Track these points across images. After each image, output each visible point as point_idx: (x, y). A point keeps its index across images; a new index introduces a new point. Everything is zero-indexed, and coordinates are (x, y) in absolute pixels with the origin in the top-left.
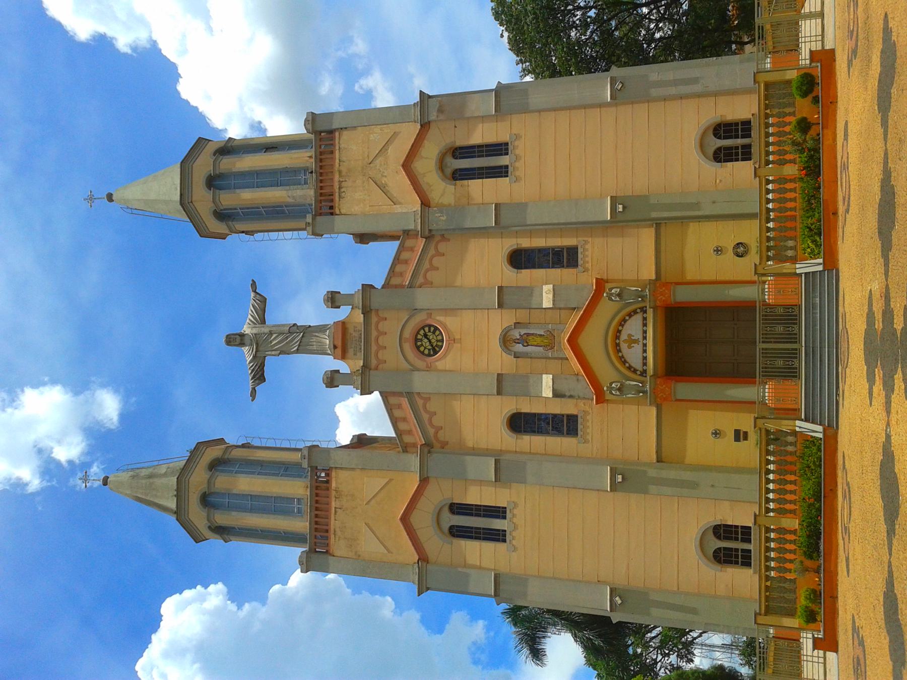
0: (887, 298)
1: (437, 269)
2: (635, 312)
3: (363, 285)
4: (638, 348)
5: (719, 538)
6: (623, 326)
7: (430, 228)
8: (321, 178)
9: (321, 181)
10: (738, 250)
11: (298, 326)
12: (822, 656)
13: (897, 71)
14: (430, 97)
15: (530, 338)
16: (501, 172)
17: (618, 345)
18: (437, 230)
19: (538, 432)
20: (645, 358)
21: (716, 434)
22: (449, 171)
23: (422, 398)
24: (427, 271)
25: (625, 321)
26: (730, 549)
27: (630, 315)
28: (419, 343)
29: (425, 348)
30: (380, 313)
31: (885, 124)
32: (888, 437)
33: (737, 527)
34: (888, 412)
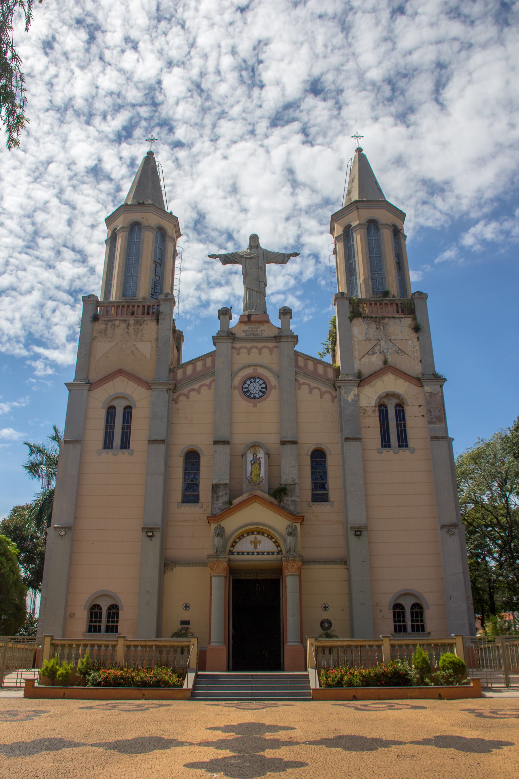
0: (290, 743)
1: (310, 393)
2: (278, 546)
3: (297, 336)
4: (250, 548)
5: (109, 609)
6: (268, 537)
7: (342, 387)
8: (378, 304)
9: (376, 304)
10: (326, 623)
11: (265, 288)
12: (22, 686)
13: (469, 753)
14: (441, 386)
15: (258, 466)
16: (386, 443)
17: (253, 533)
18: (340, 393)
19: (185, 473)
20: (243, 554)
21: (186, 607)
22: (386, 401)
23: (211, 383)
24: (309, 385)
25: (271, 538)
26: (101, 617)
27: (275, 542)
28: (252, 380)
29: (249, 385)
30: (275, 350)
31: (426, 742)
32: (182, 744)
33: (117, 622)
34: (200, 744)
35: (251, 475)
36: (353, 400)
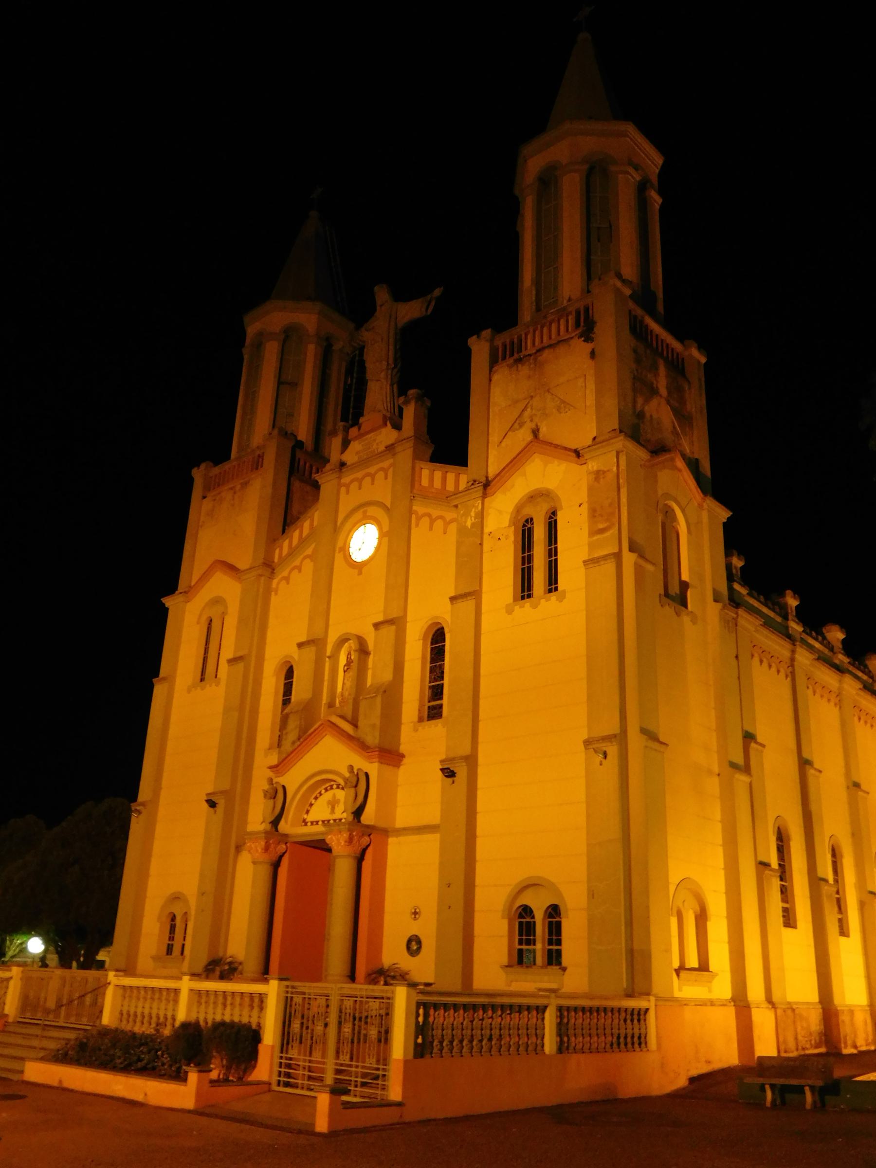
7: (459, 506)
35: (343, 690)
36: (473, 525)
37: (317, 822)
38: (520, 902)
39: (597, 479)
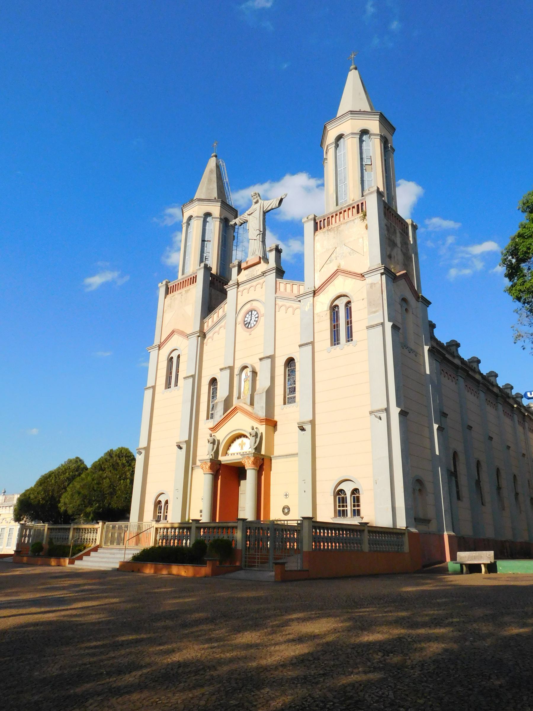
10: (286, 509)
37: (234, 454)
38: (340, 488)
39: (371, 287)
